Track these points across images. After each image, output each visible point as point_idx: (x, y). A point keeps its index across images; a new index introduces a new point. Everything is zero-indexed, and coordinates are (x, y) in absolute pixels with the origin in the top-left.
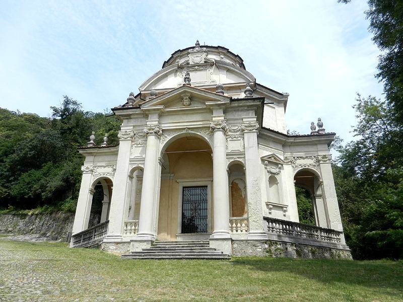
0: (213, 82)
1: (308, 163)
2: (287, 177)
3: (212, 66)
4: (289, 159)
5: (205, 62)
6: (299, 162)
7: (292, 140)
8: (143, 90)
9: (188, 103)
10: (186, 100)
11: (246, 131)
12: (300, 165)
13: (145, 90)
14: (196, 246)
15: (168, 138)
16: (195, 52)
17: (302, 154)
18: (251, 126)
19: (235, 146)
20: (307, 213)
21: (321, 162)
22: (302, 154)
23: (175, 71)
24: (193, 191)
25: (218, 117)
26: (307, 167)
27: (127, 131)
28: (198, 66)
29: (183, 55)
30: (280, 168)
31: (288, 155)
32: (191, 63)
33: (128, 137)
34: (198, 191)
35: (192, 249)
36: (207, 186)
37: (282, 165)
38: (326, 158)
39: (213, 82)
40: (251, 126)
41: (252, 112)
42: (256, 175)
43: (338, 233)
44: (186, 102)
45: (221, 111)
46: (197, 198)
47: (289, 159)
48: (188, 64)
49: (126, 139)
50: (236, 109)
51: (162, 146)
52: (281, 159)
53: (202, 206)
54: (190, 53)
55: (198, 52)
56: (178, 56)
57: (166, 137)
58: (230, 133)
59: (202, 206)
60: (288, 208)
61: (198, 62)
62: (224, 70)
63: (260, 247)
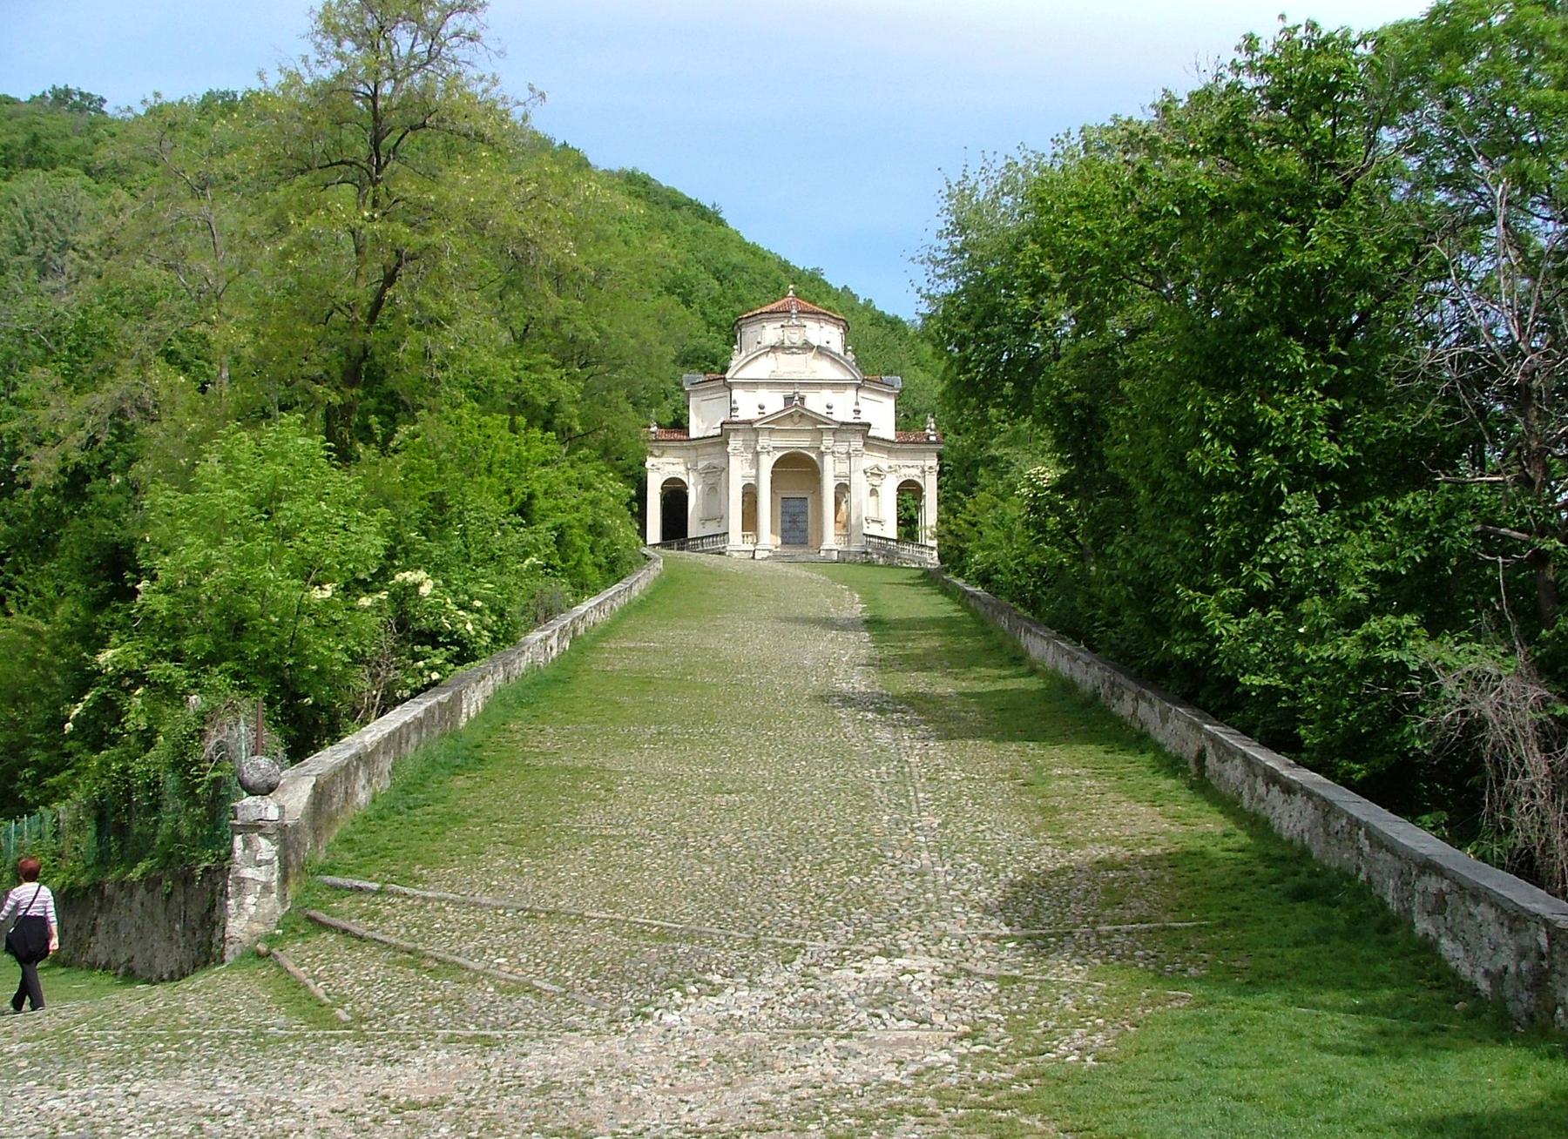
1: (913, 473)
6: (905, 471)
15: (779, 454)
17: (910, 463)
19: (842, 468)
20: (908, 525)
22: (910, 463)
24: (791, 503)
25: (828, 441)
31: (893, 462)
32: (787, 343)
34: (797, 503)
42: (860, 486)
44: (796, 419)
50: (845, 431)
53: (801, 518)
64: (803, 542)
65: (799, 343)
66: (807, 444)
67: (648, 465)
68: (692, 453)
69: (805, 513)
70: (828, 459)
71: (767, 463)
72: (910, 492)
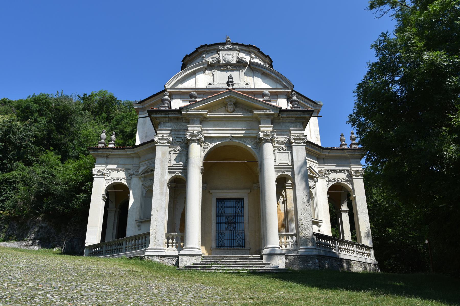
0: (247, 84)
2: (321, 189)
3: (244, 67)
4: (323, 173)
5: (238, 62)
6: (333, 176)
7: (326, 153)
8: (169, 87)
9: (232, 109)
10: (230, 106)
11: (294, 144)
12: (334, 179)
13: (171, 88)
14: (249, 261)
15: (211, 145)
16: (226, 50)
18: (300, 139)
21: (354, 177)
23: (204, 69)
24: (227, 203)
25: (266, 129)
26: (340, 182)
27: (165, 135)
28: (230, 65)
29: (210, 51)
30: (315, 182)
32: (222, 61)
33: (165, 143)
34: (233, 203)
35: (246, 264)
36: (243, 199)
37: (317, 178)
38: (359, 173)
39: (247, 84)
40: (300, 139)
41: (299, 124)
43: (369, 248)
44: (230, 108)
45: (269, 121)
46: (233, 211)
47: (323, 173)
48: (219, 62)
49: (163, 145)
51: (203, 154)
52: (316, 172)
53: (238, 219)
54: (220, 50)
55: (230, 49)
56: (204, 51)
57: (208, 145)
58: (277, 145)
59: (238, 219)
60: (322, 224)
61: (230, 61)
62: (259, 72)
63: (311, 262)
64: (239, 246)
65: (235, 61)
66: (241, 133)
67: (94, 171)
68: (136, 160)
69: (242, 215)
70: (268, 148)
71: (197, 153)
72: (339, 196)
